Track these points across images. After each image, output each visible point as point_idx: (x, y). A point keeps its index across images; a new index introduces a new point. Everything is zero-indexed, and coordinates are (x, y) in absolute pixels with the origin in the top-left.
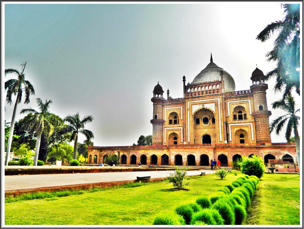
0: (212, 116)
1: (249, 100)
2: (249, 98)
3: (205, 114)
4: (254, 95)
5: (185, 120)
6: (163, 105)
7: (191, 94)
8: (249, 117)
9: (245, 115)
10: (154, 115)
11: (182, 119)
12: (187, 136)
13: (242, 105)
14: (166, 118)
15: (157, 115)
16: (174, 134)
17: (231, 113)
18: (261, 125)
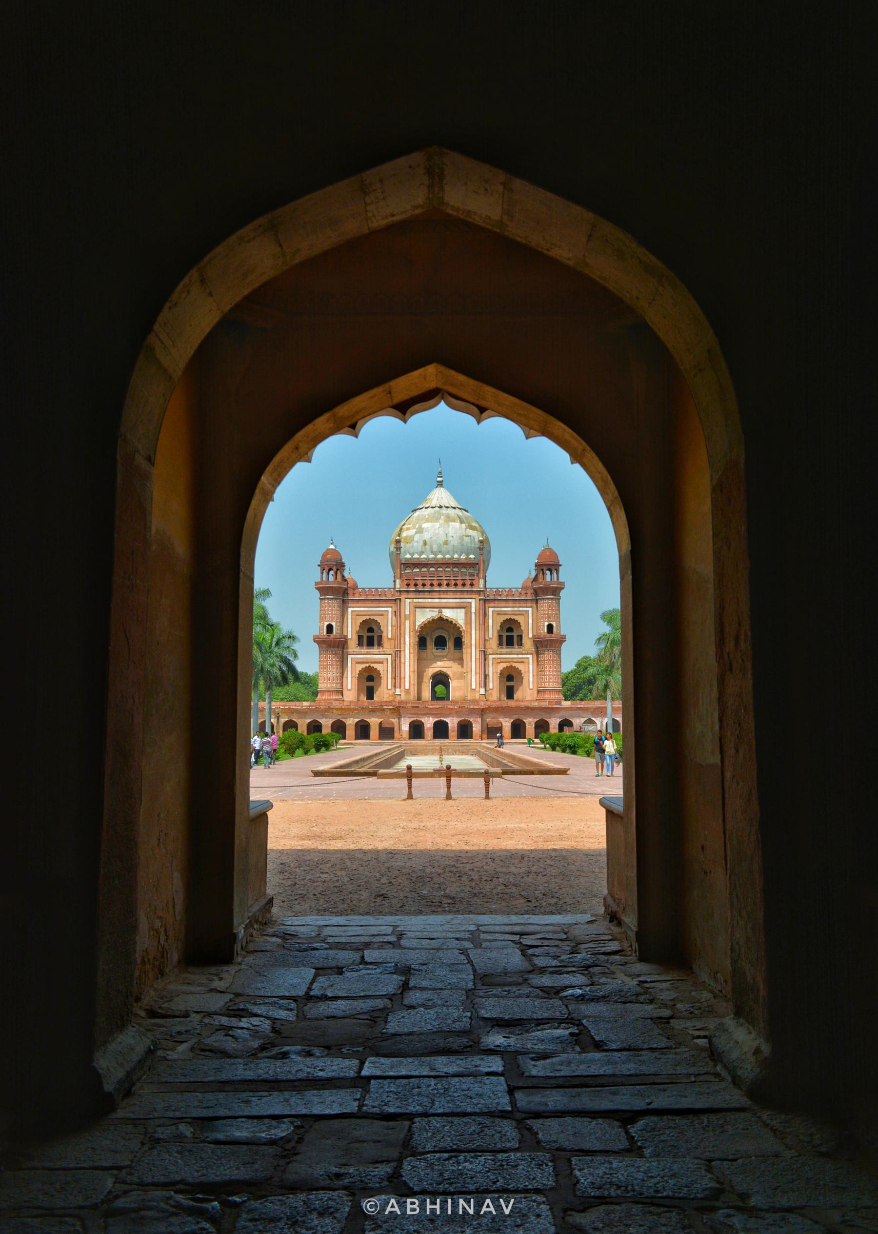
0: (453, 634)
1: (530, 609)
2: (529, 605)
3: (442, 629)
4: (540, 602)
5: (398, 637)
6: (343, 600)
7: (413, 582)
8: (528, 644)
9: (520, 637)
10: (326, 624)
11: (390, 636)
12: (402, 676)
13: (516, 618)
14: (351, 631)
15: (334, 624)
16: (369, 669)
17: (496, 634)
18: (549, 660)
